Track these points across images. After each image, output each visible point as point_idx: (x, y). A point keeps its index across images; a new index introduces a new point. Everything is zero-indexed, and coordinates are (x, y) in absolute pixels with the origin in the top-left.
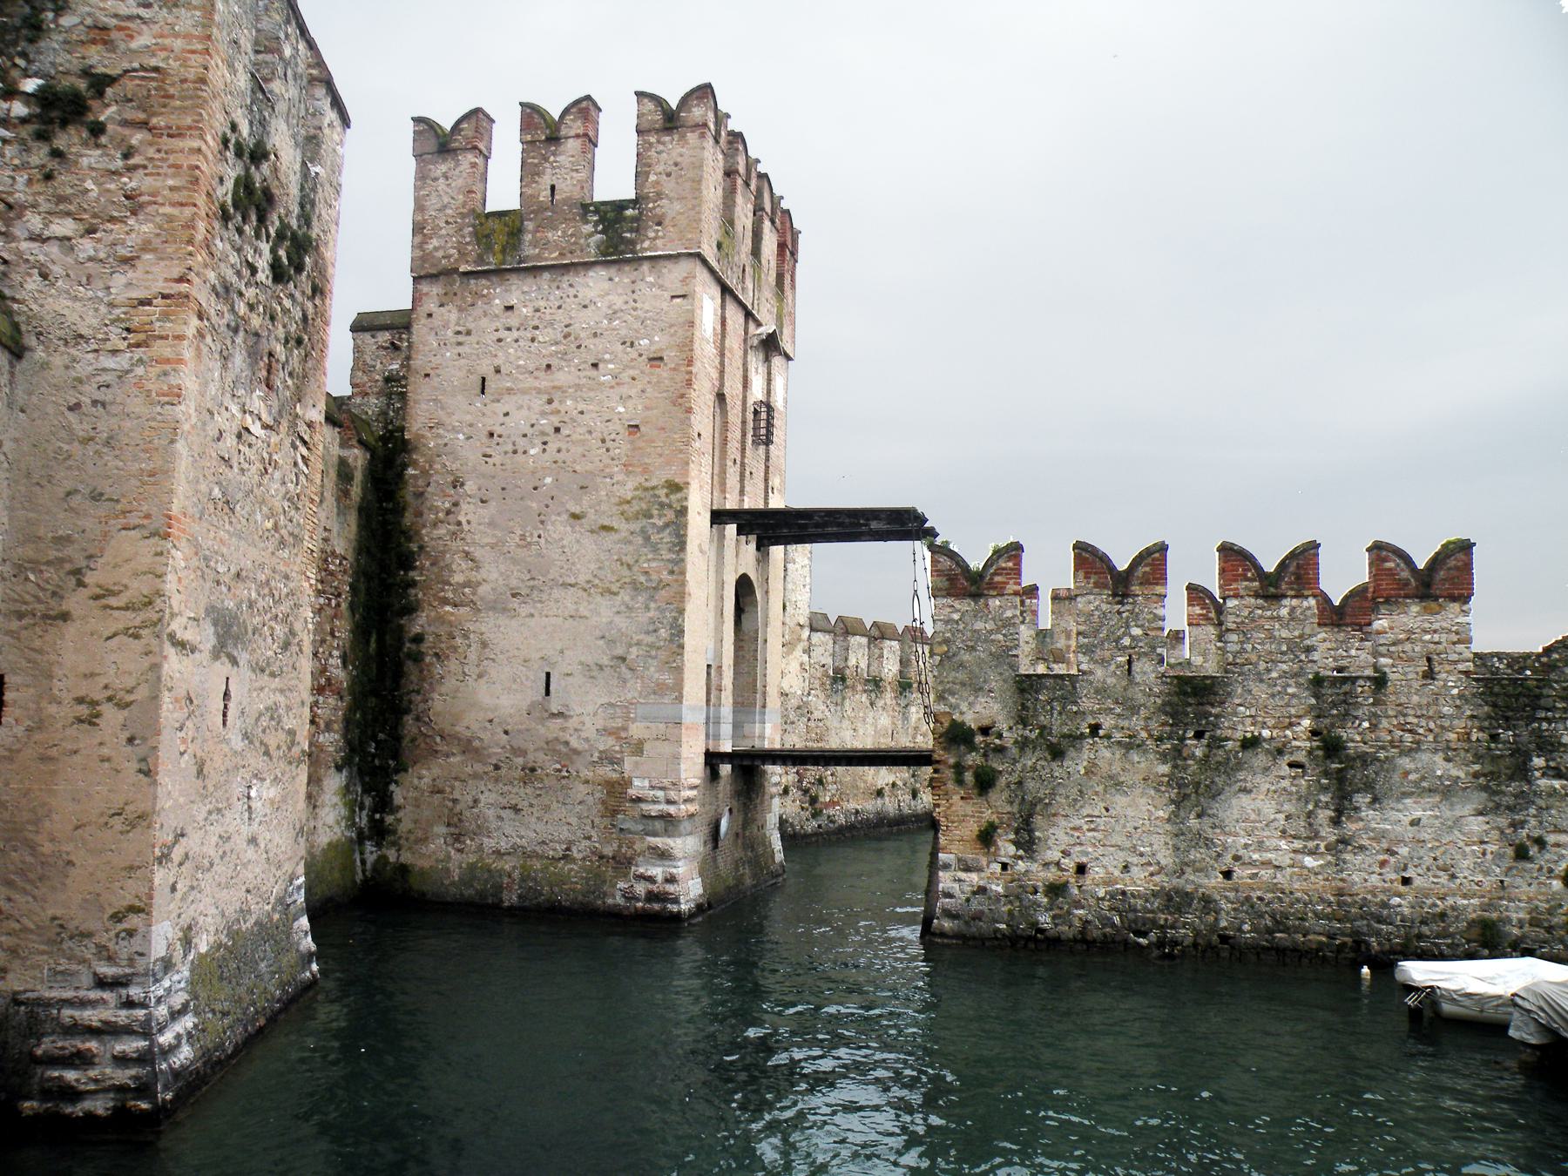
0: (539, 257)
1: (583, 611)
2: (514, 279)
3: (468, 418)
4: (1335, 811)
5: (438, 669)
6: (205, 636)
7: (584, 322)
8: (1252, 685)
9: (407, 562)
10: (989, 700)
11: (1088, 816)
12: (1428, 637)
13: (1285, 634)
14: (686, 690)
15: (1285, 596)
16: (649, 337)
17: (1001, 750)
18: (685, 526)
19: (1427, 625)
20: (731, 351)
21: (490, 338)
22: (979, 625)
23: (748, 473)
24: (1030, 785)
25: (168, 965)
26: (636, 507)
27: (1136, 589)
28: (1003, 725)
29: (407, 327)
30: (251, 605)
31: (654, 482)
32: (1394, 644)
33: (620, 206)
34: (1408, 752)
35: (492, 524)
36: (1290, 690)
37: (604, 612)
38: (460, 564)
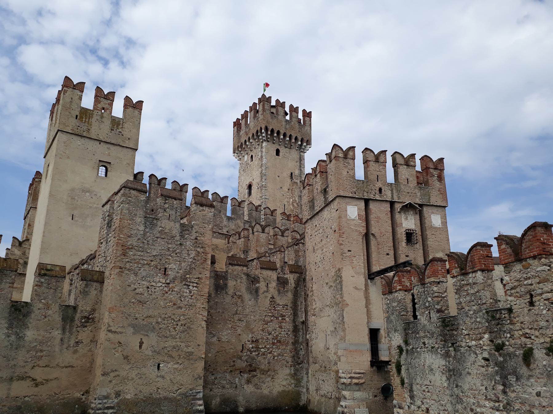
1: (330, 314)
3: (312, 259)
4: (503, 385)
10: (398, 334)
11: (426, 385)
12: (526, 282)
13: (472, 291)
14: (346, 338)
15: (470, 273)
19: (525, 276)
20: (378, 218)
24: (410, 370)
25: (107, 397)
26: (335, 278)
27: (427, 280)
32: (512, 289)
36: (478, 320)
38: (314, 304)
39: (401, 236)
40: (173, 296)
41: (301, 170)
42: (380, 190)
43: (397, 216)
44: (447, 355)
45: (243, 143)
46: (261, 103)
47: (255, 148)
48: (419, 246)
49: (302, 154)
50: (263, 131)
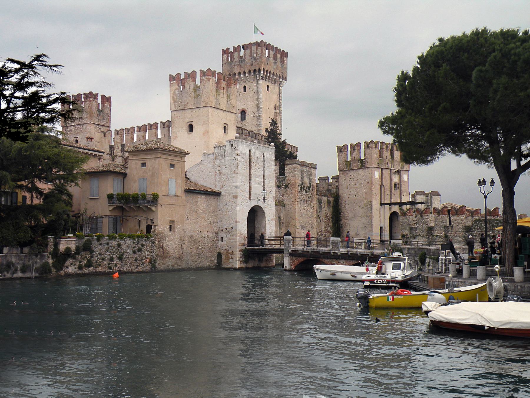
0: (353, 168)
1: (361, 220)
2: (351, 171)
3: (346, 192)
5: (344, 229)
6: (300, 228)
7: (359, 177)
8: (437, 228)
9: (340, 214)
13: (441, 220)
14: (373, 231)
16: (367, 179)
17: (408, 237)
18: (372, 207)
20: (385, 177)
21: (348, 180)
22: (405, 220)
23: (393, 195)
26: (367, 204)
27: (423, 214)
28: (408, 234)
29: (338, 178)
30: (306, 224)
31: (368, 201)
33: (363, 160)
34: (455, 237)
35: (350, 208)
37: (363, 220)
39: (393, 186)
40: (308, 212)
41: (280, 102)
42: (387, 163)
43: (392, 175)
44: (428, 238)
45: (237, 74)
46: (260, 47)
47: (249, 81)
48: (398, 190)
49: (281, 88)
50: (262, 72)
